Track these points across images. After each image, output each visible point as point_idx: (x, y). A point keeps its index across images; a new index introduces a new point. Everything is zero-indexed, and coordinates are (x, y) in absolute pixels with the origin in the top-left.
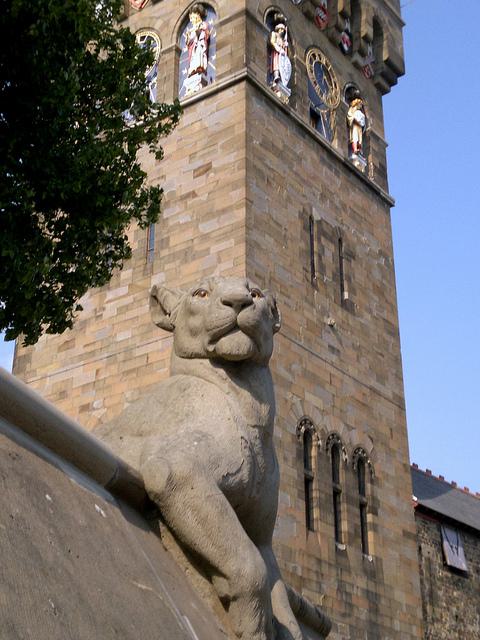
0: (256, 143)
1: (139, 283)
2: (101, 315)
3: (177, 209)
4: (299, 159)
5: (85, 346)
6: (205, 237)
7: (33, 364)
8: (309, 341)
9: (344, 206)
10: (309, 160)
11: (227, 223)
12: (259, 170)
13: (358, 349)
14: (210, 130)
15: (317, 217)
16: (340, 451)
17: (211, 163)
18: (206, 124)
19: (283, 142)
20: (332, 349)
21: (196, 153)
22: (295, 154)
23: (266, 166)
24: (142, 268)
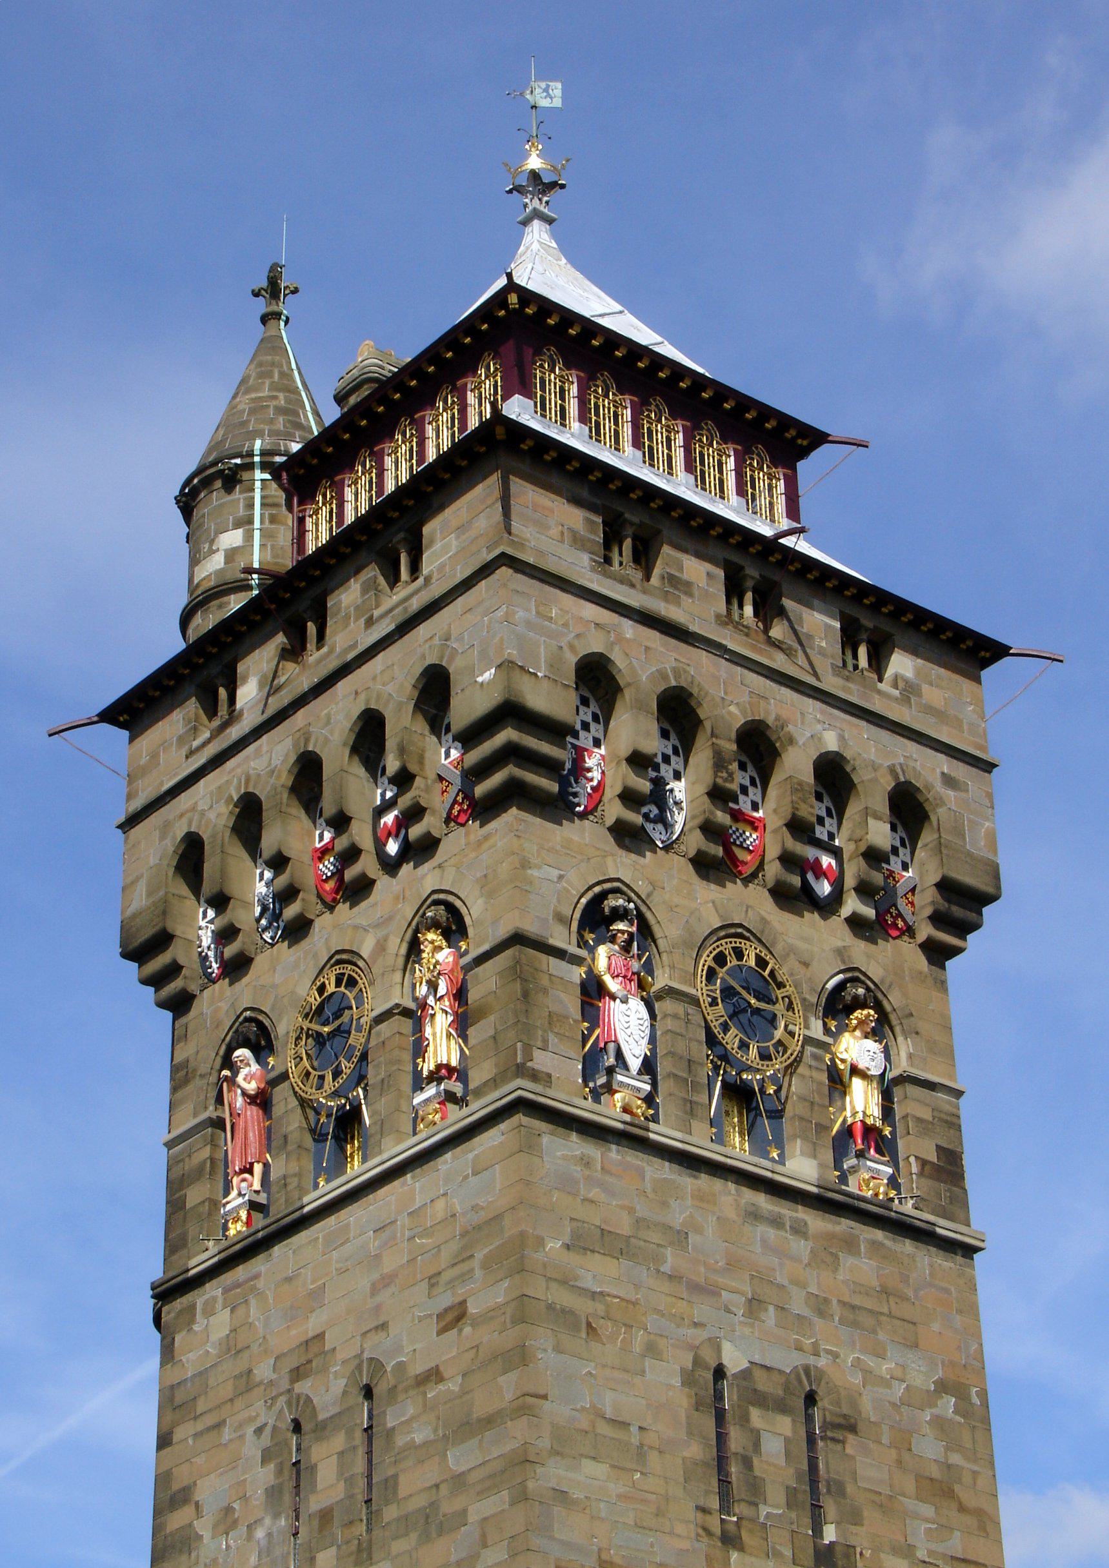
6: (459, 1481)
15: (734, 1359)
17: (465, 1301)
19: (631, 1210)
22: (667, 1228)
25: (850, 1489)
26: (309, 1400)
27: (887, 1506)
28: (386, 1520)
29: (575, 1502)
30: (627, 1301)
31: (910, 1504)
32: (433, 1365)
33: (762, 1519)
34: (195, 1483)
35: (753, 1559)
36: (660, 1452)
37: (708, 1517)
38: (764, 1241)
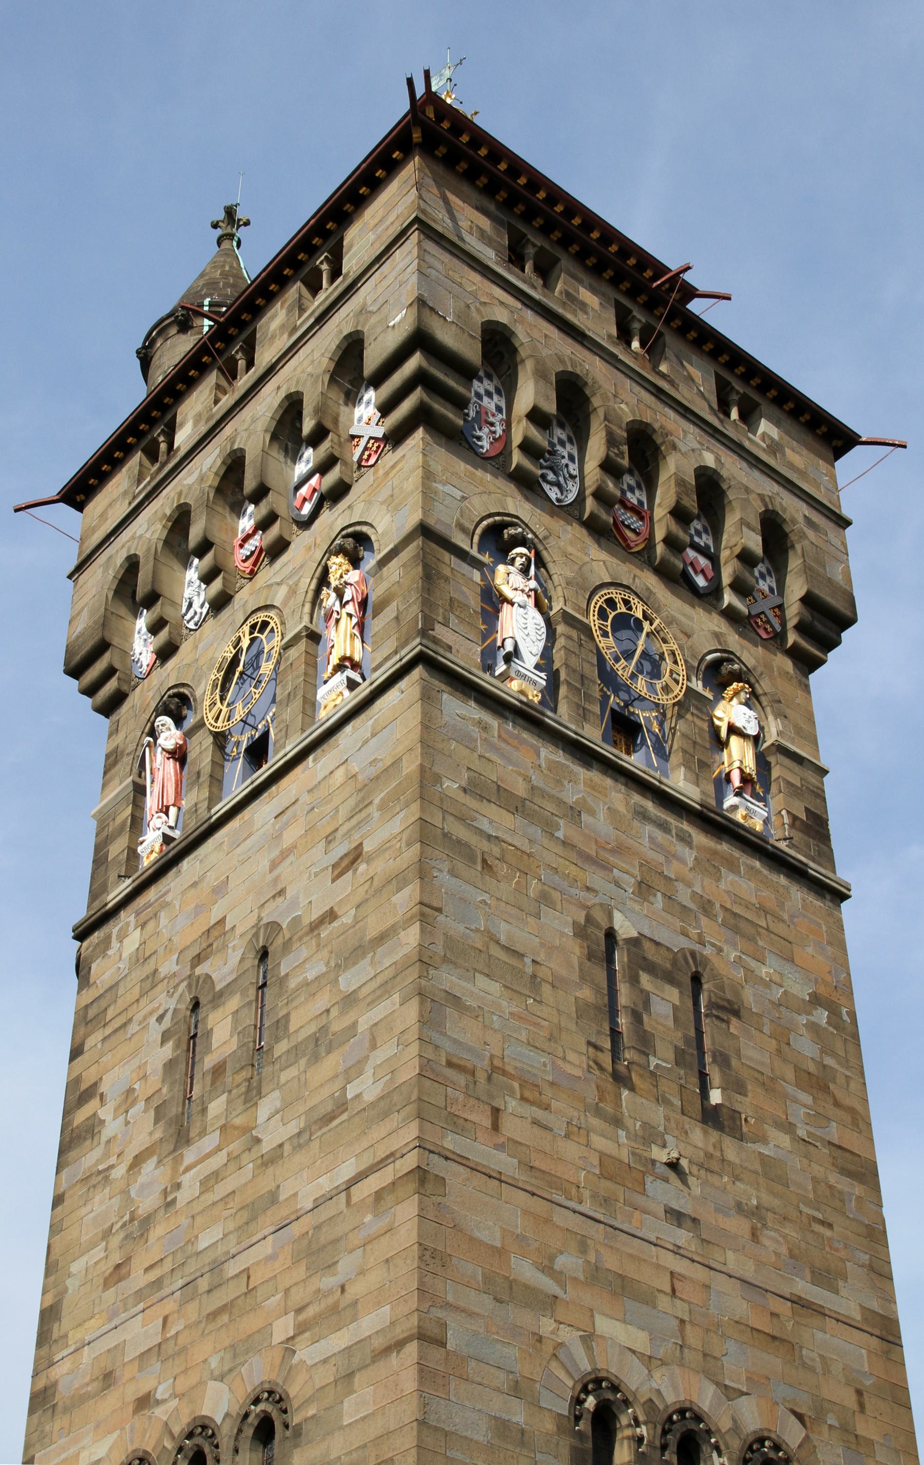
0: (451, 786)
1: (238, 1121)
2: (174, 1201)
3: (304, 953)
4: (574, 813)
5: (147, 1270)
6: (349, 1000)
7: (64, 1321)
8: (607, 1202)
9: (706, 907)
10: (602, 815)
11: (387, 962)
12: (459, 842)
13: (756, 1213)
14: (360, 777)
15: (625, 928)
16: (705, 1448)
17: (361, 844)
18: (355, 767)
19: (527, 779)
20: (676, 1217)
21: (336, 830)
22: (560, 802)
23: (480, 832)
24: (243, 1089)
25: (734, 1062)
26: (208, 977)
27: (769, 1085)
28: (275, 1056)
29: (468, 1008)
30: (522, 852)
31: (790, 1089)
32: (327, 908)
33: (652, 1068)
34: (101, 1079)
35: (643, 1100)
36: (553, 987)
37: (599, 1054)
38: (652, 839)
